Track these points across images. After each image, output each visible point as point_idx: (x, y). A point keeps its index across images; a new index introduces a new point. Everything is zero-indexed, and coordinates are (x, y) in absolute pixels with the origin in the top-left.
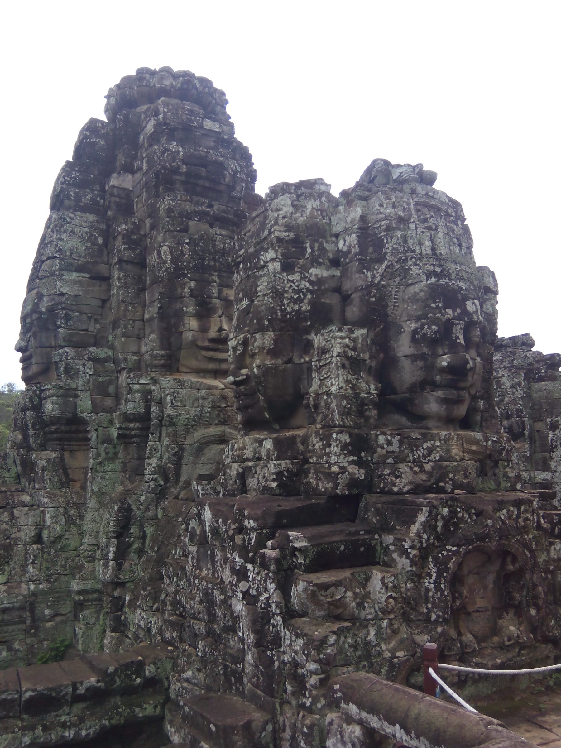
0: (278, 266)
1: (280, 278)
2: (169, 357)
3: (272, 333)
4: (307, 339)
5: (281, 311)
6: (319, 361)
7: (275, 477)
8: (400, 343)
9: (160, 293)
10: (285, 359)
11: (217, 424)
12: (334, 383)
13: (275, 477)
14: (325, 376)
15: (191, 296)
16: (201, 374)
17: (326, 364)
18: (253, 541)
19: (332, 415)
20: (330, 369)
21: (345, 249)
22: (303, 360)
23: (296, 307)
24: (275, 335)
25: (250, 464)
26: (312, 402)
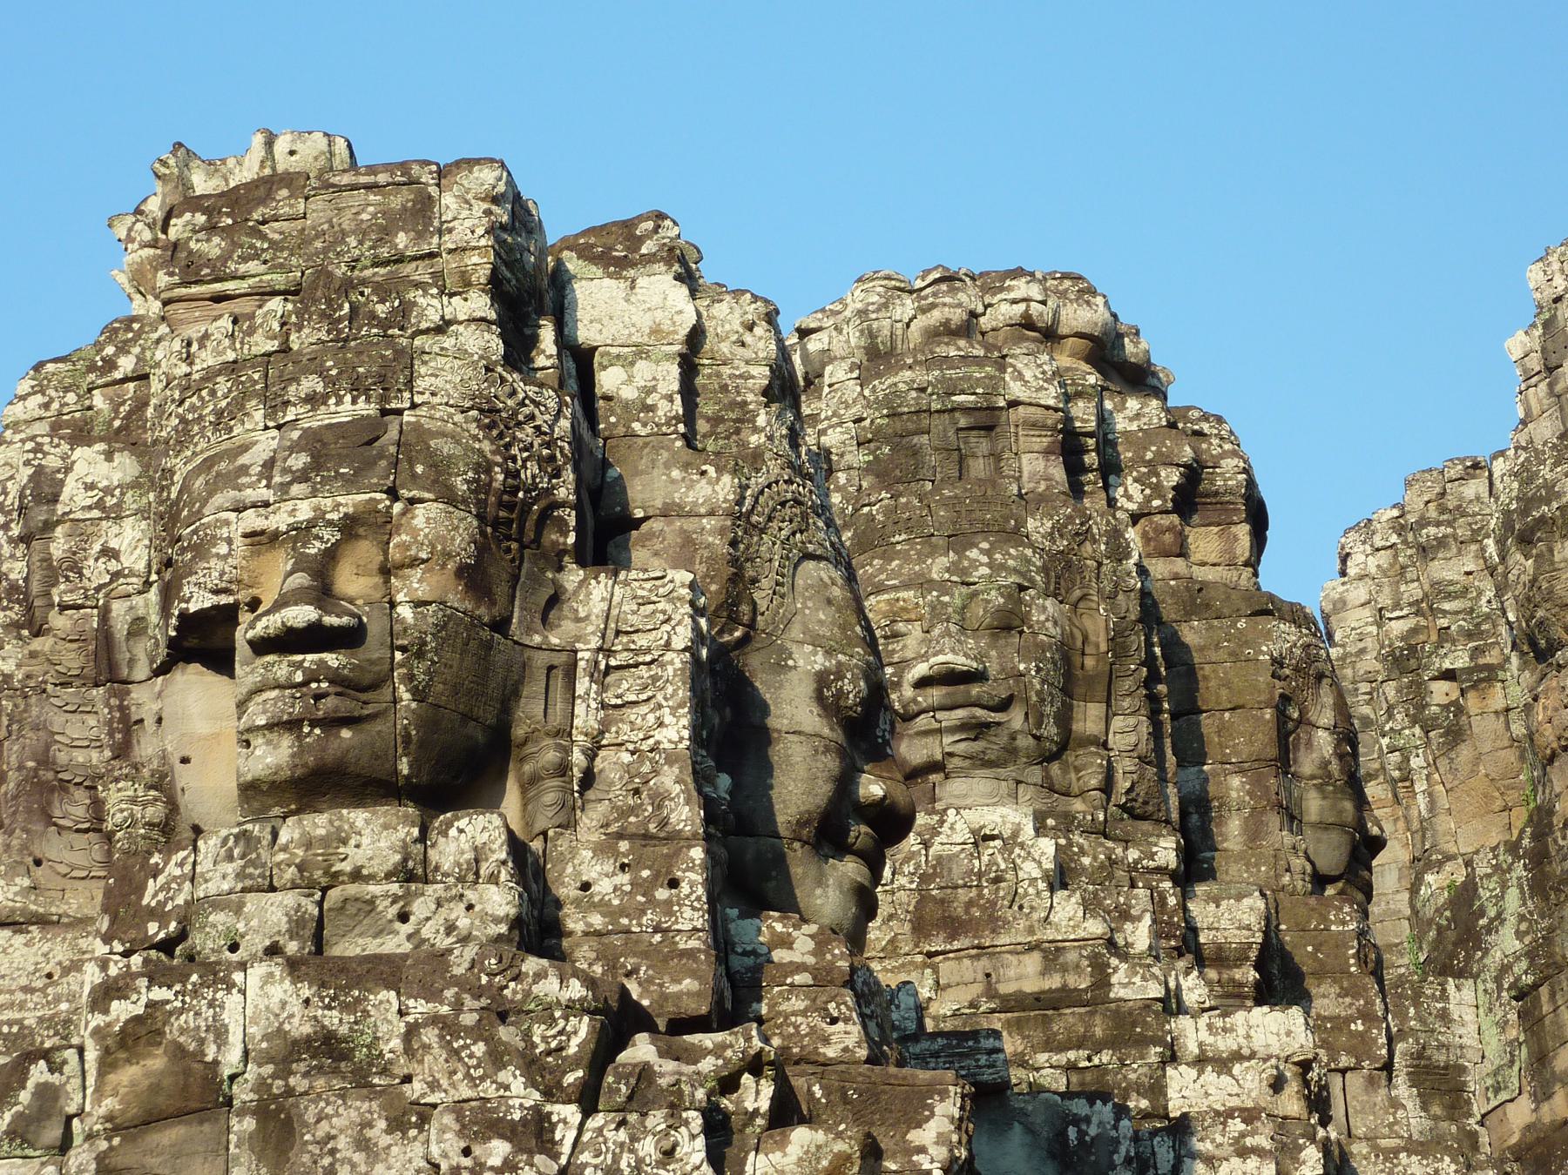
7: (503, 929)
8: (785, 693)
12: (668, 719)
13: (503, 929)
14: (633, 698)
18: (575, 1042)
21: (628, 393)
22: (537, 639)
25: (374, 889)
26: (577, 757)
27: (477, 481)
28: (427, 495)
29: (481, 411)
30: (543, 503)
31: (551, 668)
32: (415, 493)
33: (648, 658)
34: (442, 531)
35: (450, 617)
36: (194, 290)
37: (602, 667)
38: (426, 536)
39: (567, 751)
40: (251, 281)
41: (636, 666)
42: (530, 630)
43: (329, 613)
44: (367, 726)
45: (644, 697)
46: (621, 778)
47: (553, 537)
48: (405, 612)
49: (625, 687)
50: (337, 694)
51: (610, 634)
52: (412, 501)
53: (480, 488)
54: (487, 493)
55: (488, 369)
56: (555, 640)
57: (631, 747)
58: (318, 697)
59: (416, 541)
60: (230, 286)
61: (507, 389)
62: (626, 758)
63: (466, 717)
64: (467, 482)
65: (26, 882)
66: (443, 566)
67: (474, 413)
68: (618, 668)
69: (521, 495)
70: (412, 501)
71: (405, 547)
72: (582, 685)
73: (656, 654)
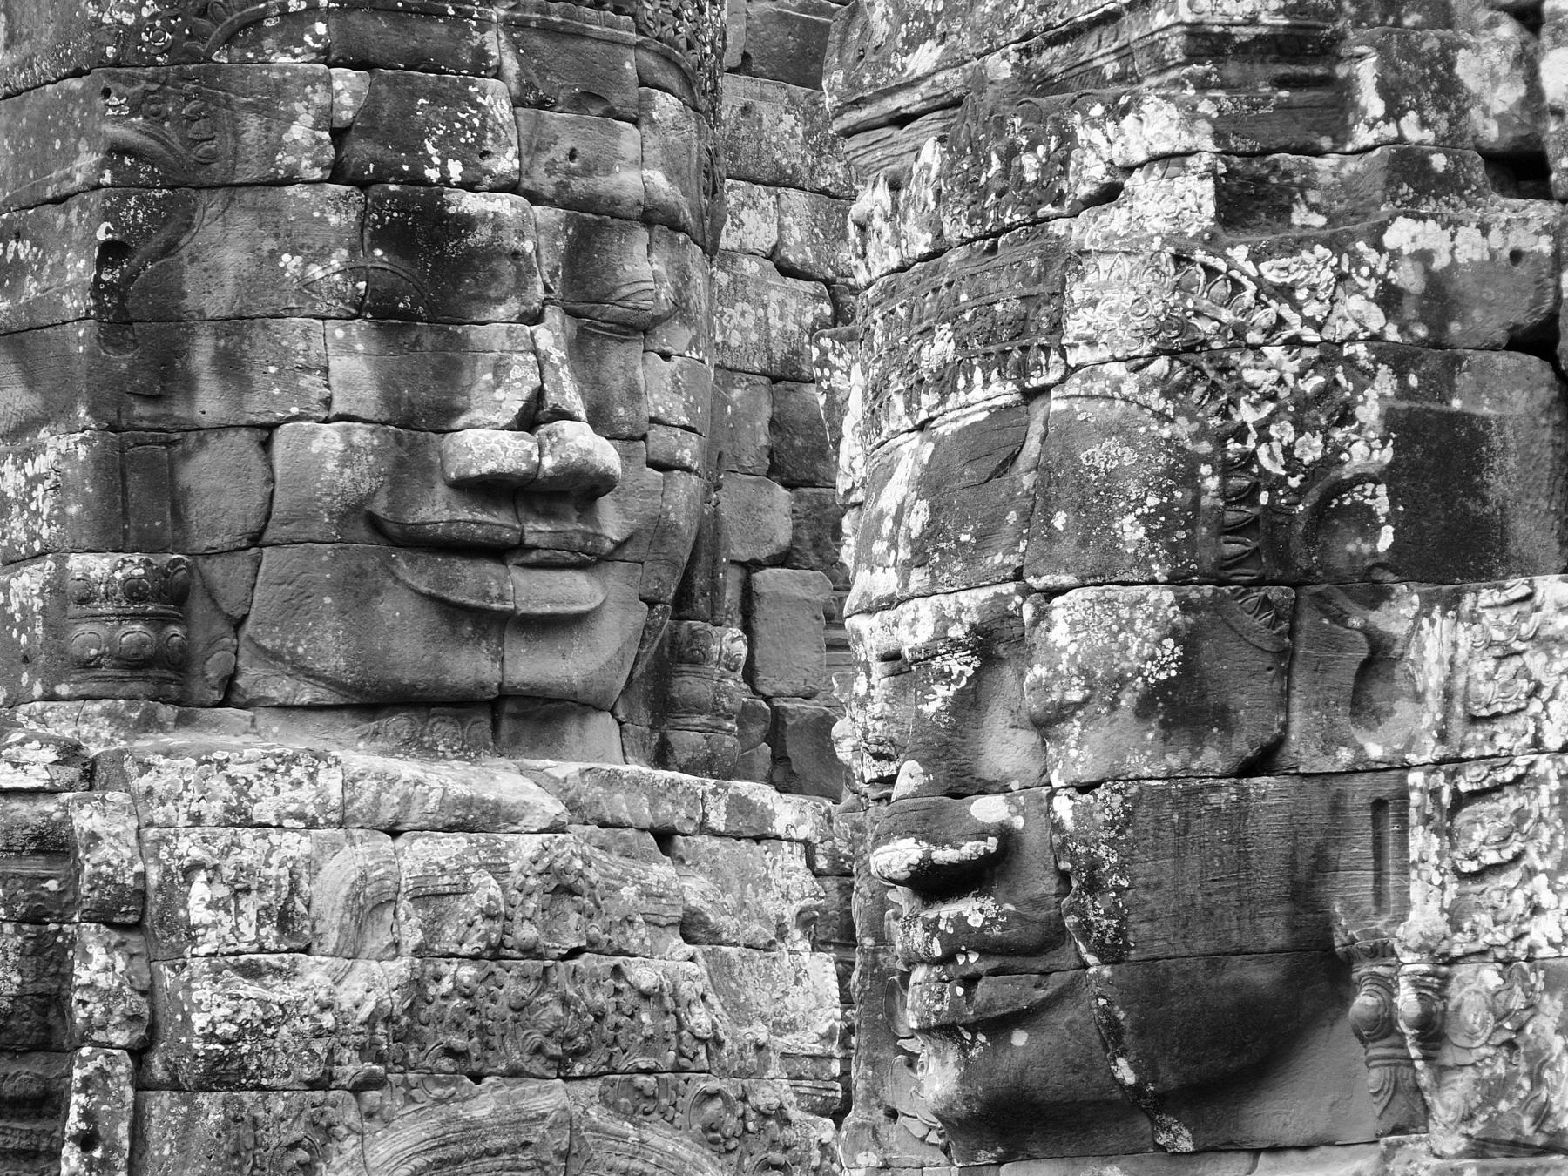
0: (1196, 198)
1: (1211, 272)
2: (166, 597)
3: (1168, 596)
4: (1368, 632)
5: (1226, 469)
6: (1453, 763)
9: (118, 150)
10: (1242, 746)
11: (515, 1073)
12: (1546, 898)
14: (1491, 857)
15: (337, 173)
16: (398, 723)
17: (1498, 788)
19: (1537, 1081)
20: (1521, 815)
22: (1345, 755)
23: (1311, 449)
24: (1186, 606)
26: (1407, 1001)
27: (1161, 509)
28: (1066, 579)
29: (1172, 354)
30: (1314, 494)
31: (1379, 805)
32: (1047, 580)
33: (1509, 775)
34: (1100, 638)
35: (1137, 800)
36: (864, 114)
37: (1446, 799)
38: (1072, 659)
39: (1387, 986)
40: (923, 88)
41: (1498, 788)
42: (1329, 744)
43: (941, 844)
44: (1052, 1017)
45: (1507, 855)
46: (1484, 1024)
47: (1351, 547)
48: (1063, 807)
49: (1481, 831)
50: (994, 972)
51: (1457, 728)
52: (1052, 593)
53: (1162, 524)
54: (1191, 524)
55: (1180, 259)
56: (1375, 751)
57: (1501, 954)
58: (970, 982)
59: (1057, 675)
60: (900, 102)
61: (1221, 289)
62: (1490, 977)
63: (1214, 960)
64: (1145, 519)
65: (874, 1160)
66: (1114, 705)
67: (1160, 365)
68: (1475, 796)
69: (1264, 498)
70: (1052, 593)
71: (1043, 687)
72: (1421, 841)
73: (1521, 761)
